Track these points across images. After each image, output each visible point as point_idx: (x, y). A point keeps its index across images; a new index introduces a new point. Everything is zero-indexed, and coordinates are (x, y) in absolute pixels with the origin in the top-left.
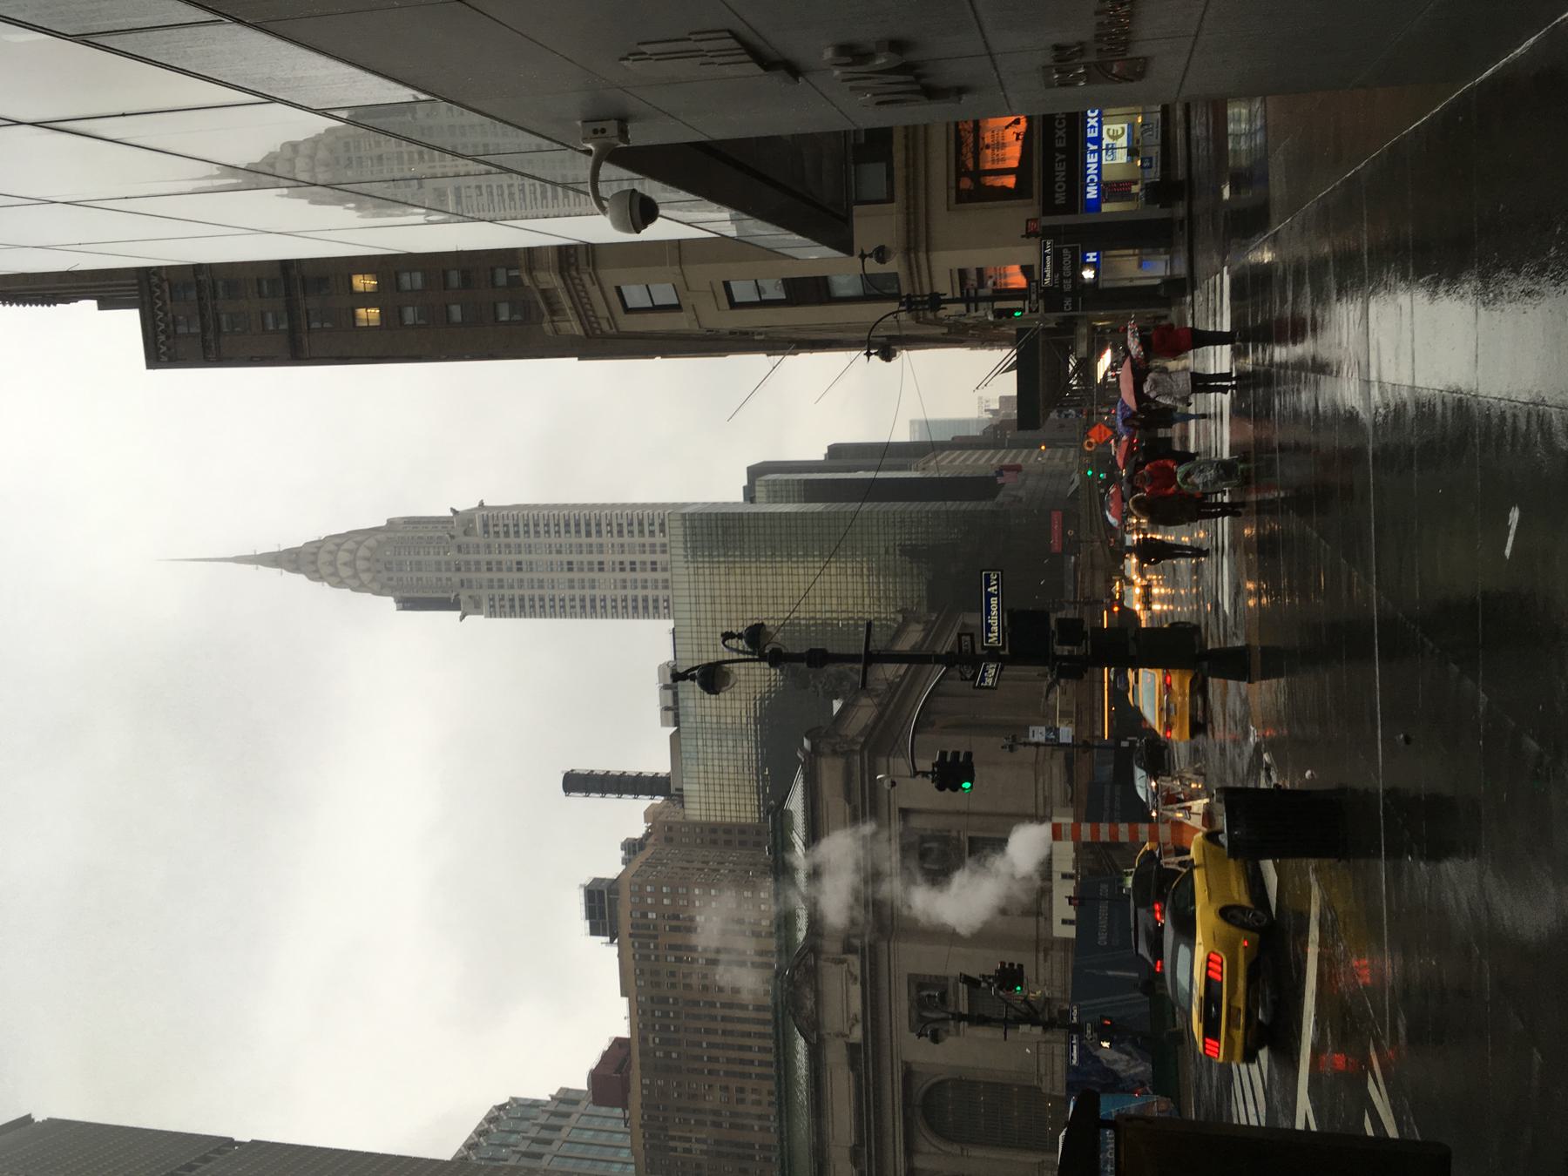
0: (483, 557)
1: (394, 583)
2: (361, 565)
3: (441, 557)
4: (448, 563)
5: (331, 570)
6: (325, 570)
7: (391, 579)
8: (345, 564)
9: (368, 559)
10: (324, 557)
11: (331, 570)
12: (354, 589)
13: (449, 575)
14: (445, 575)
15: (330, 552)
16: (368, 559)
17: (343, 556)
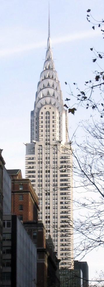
0: (52, 156)
1: (40, 115)
2: (48, 99)
3: (52, 137)
4: (49, 140)
5: (46, 85)
6: (45, 83)
7: (42, 113)
8: (48, 92)
9: (50, 103)
10: (51, 82)
11: (46, 85)
12: (37, 94)
13: (44, 140)
14: (44, 138)
15: (53, 86)
16: (50, 103)
17: (51, 91)
